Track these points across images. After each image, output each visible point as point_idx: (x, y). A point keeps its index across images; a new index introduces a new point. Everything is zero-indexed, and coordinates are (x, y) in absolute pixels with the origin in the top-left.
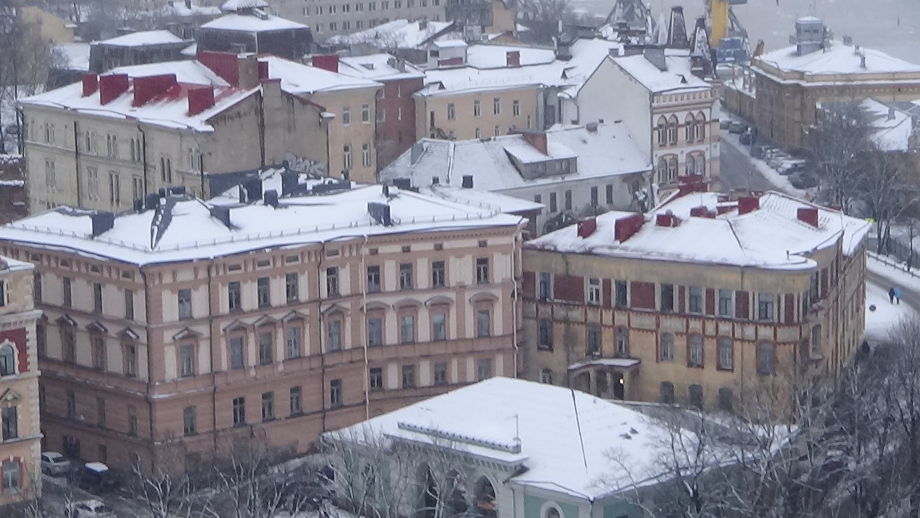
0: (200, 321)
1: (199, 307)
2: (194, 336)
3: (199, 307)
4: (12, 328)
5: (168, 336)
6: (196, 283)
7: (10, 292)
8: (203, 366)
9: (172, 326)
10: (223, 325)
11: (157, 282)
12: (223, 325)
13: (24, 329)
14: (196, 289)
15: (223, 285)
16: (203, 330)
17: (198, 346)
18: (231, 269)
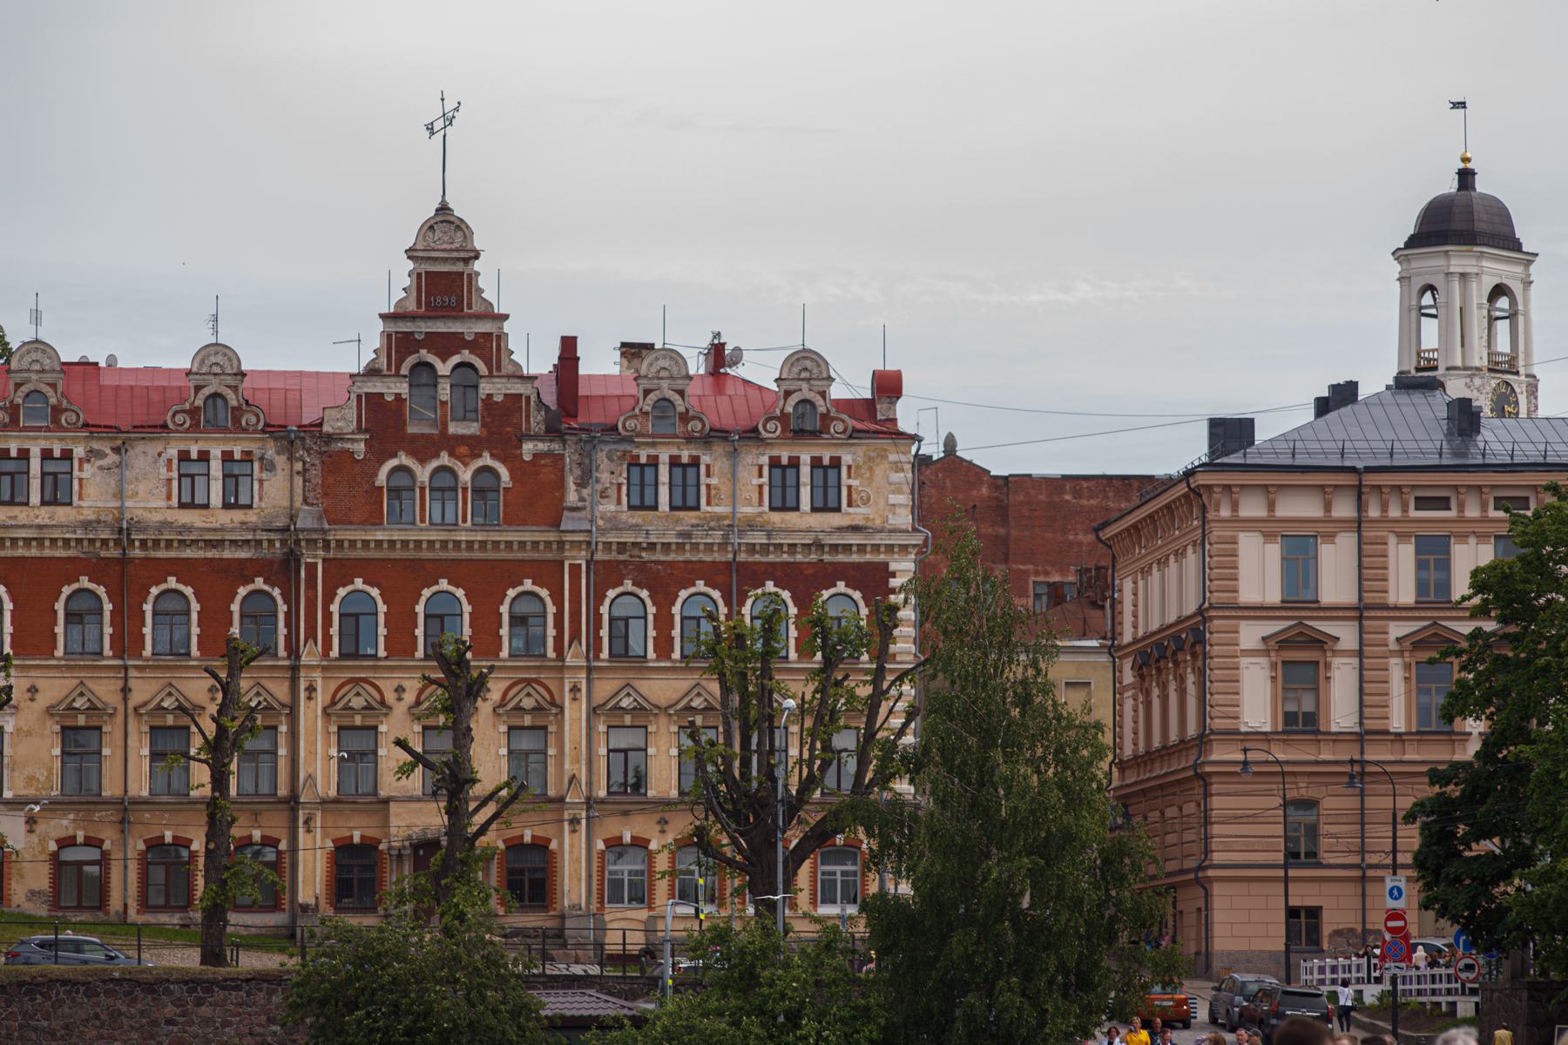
0: (1336, 612)
1: (1336, 577)
2: (1321, 643)
3: (1336, 577)
4: (855, 558)
5: (1251, 634)
6: (1327, 529)
7: (854, 483)
8: (1342, 713)
9: (1259, 612)
10: (1397, 630)
11: (1225, 512)
12: (1397, 630)
13: (886, 565)
14: (1330, 537)
15: (1402, 537)
16: (1346, 634)
17: (1328, 666)
18: (1422, 503)
